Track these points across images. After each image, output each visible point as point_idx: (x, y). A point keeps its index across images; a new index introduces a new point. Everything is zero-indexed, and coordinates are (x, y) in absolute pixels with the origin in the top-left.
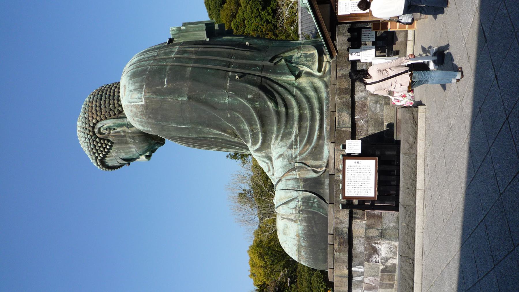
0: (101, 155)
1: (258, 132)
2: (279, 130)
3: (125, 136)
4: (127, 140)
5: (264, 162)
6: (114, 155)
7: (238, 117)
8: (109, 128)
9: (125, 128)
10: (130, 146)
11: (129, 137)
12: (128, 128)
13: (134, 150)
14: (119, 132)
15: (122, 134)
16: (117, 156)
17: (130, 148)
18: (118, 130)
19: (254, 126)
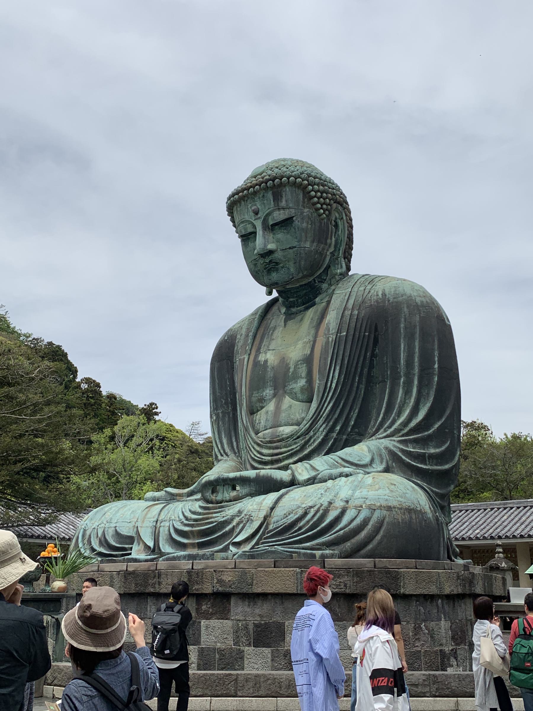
0: (313, 193)
1: (426, 464)
2: (436, 493)
3: (326, 244)
4: (322, 244)
5: (372, 461)
6: (306, 210)
7: (444, 443)
8: (336, 226)
9: (332, 249)
10: (315, 244)
11: (323, 249)
12: (331, 253)
13: (308, 245)
14: (331, 239)
15: (329, 241)
16: (302, 213)
17: (313, 242)
18: (333, 239)
19: (435, 461)
